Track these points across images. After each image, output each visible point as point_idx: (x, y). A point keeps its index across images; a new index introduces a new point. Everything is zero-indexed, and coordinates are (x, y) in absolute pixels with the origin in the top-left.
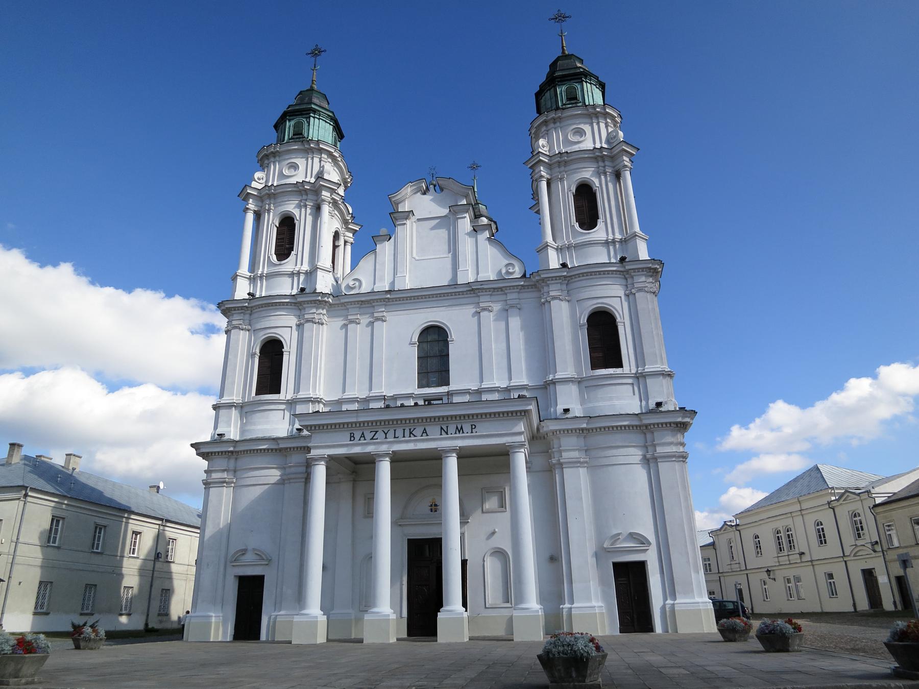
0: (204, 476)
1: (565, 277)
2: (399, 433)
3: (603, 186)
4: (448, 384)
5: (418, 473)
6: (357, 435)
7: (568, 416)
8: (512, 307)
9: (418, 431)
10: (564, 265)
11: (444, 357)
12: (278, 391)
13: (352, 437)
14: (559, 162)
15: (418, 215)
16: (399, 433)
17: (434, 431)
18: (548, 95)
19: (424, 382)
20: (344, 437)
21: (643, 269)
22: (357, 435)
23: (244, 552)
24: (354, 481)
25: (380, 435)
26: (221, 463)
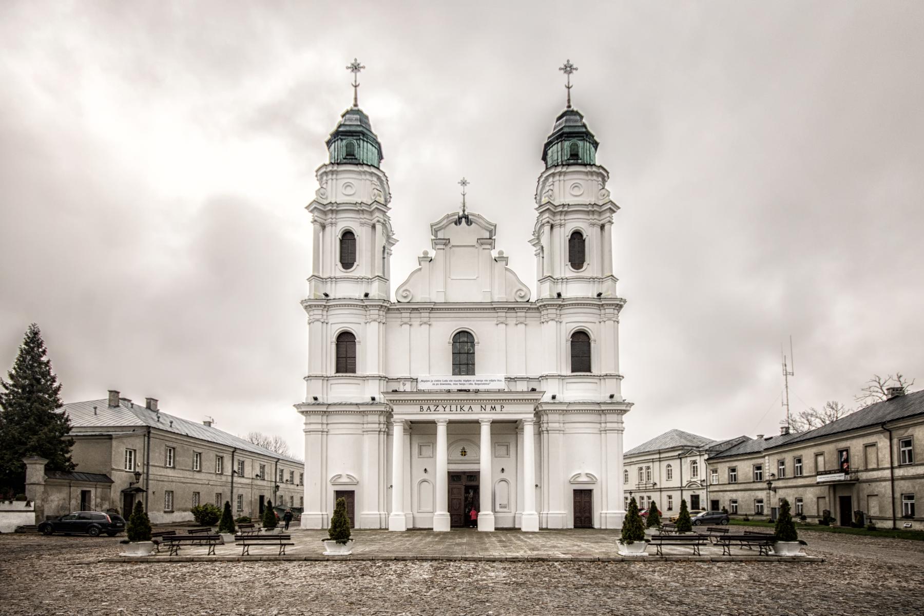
0: (304, 427)
1: (560, 305)
2: (454, 408)
3: (591, 234)
4: (473, 374)
5: (463, 433)
6: (425, 407)
7: (556, 401)
8: (521, 323)
9: (466, 408)
10: (559, 295)
11: (471, 354)
12: (354, 372)
13: (422, 408)
14: (561, 212)
15: (453, 243)
16: (454, 408)
17: (476, 408)
18: (555, 147)
19: (457, 371)
20: (417, 409)
21: (613, 305)
22: (425, 407)
23: (340, 476)
24: (411, 435)
25: (440, 408)
26: (318, 419)
